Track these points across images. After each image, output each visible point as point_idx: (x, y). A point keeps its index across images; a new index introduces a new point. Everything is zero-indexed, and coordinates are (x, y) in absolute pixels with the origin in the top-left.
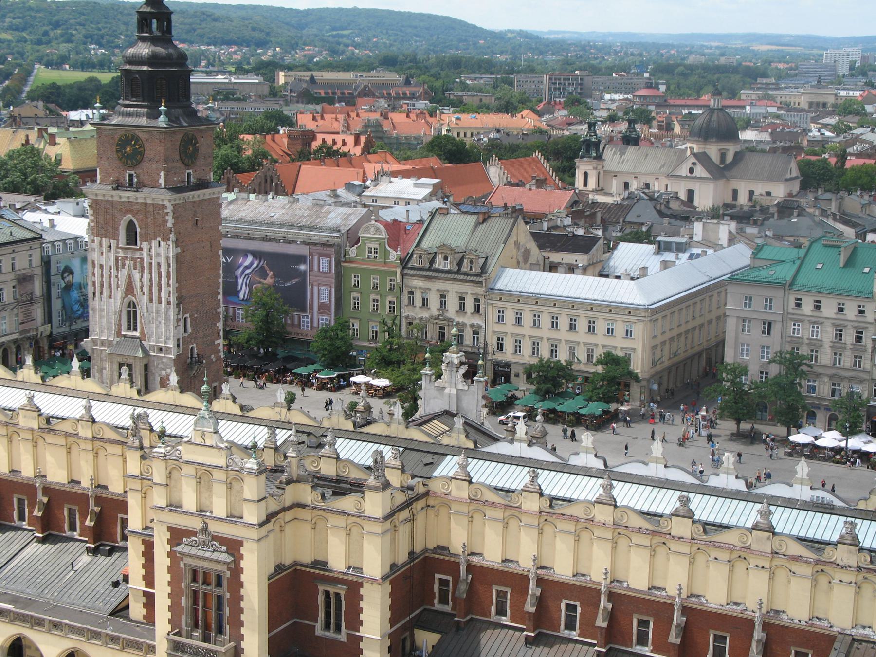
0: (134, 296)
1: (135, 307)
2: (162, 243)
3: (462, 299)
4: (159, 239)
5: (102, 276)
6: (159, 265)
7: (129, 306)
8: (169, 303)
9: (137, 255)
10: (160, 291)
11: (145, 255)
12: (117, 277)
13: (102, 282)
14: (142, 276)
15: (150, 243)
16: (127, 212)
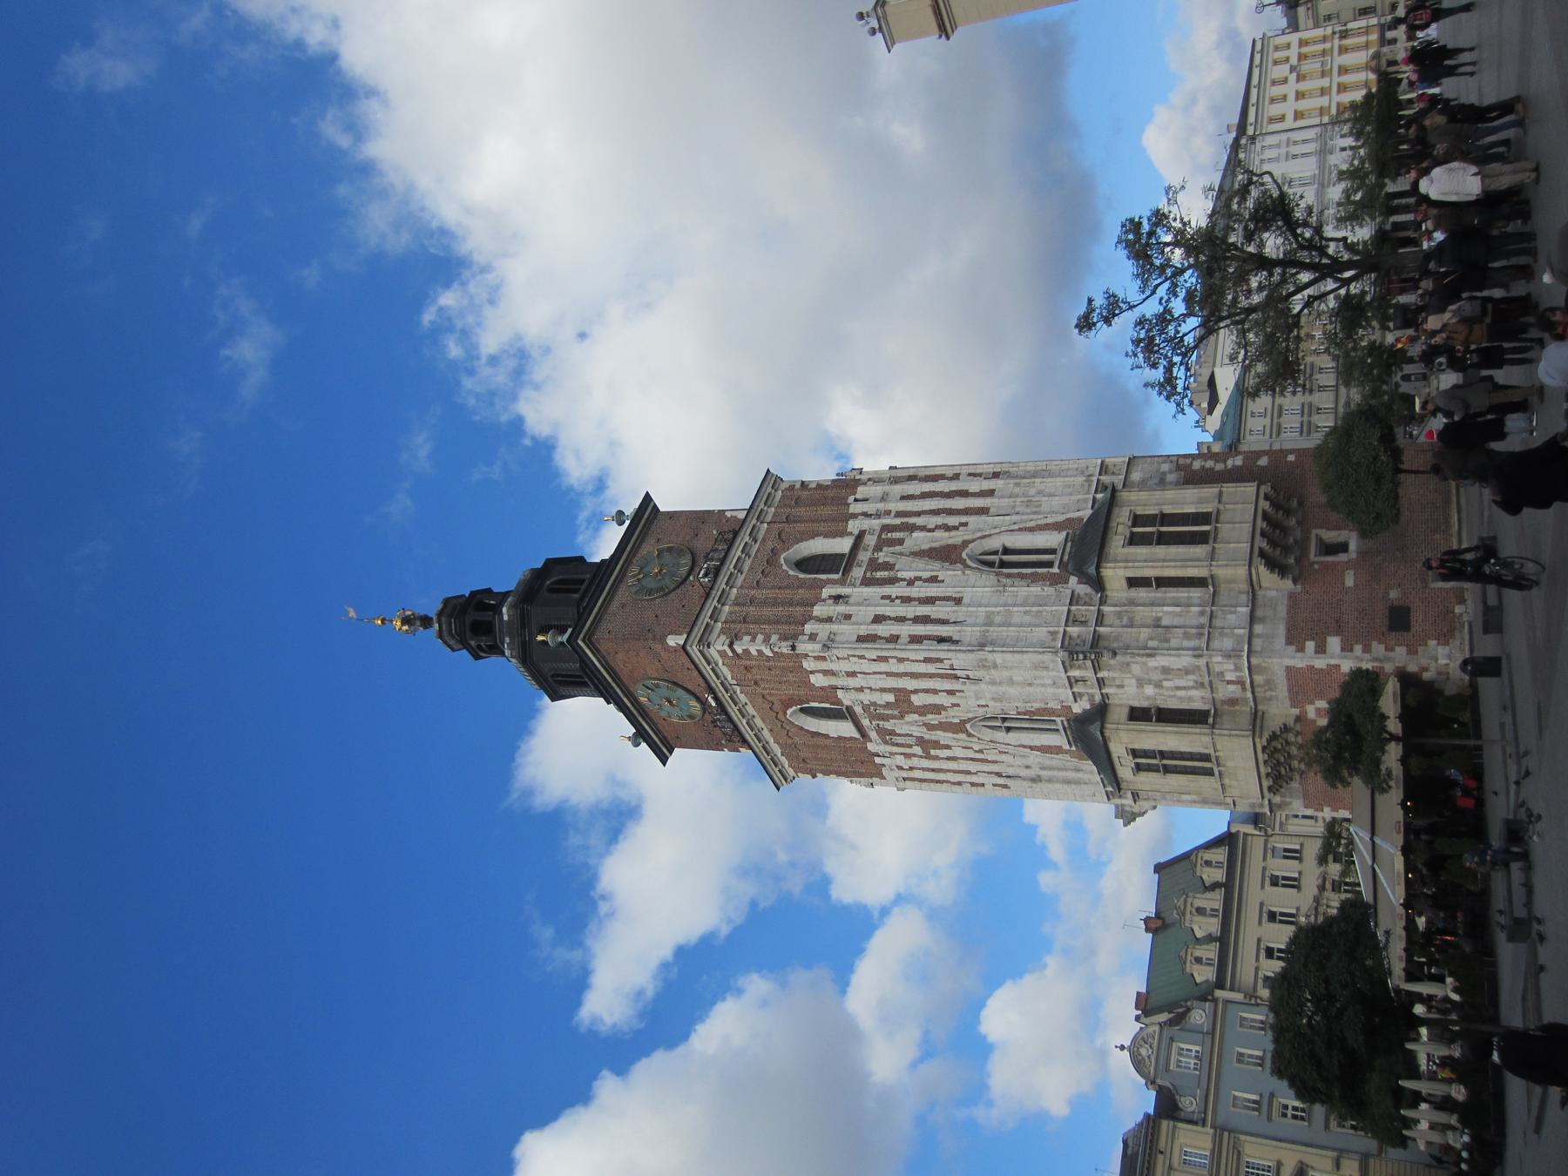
0: (965, 543)
1: (995, 553)
2: (858, 496)
3: (1275, 881)
4: (851, 499)
5: (901, 620)
6: (904, 498)
7: (991, 564)
8: (996, 475)
9: (870, 540)
10: (964, 494)
11: (876, 524)
12: (911, 583)
13: (917, 620)
14: (923, 528)
15: (855, 516)
16: (772, 560)
